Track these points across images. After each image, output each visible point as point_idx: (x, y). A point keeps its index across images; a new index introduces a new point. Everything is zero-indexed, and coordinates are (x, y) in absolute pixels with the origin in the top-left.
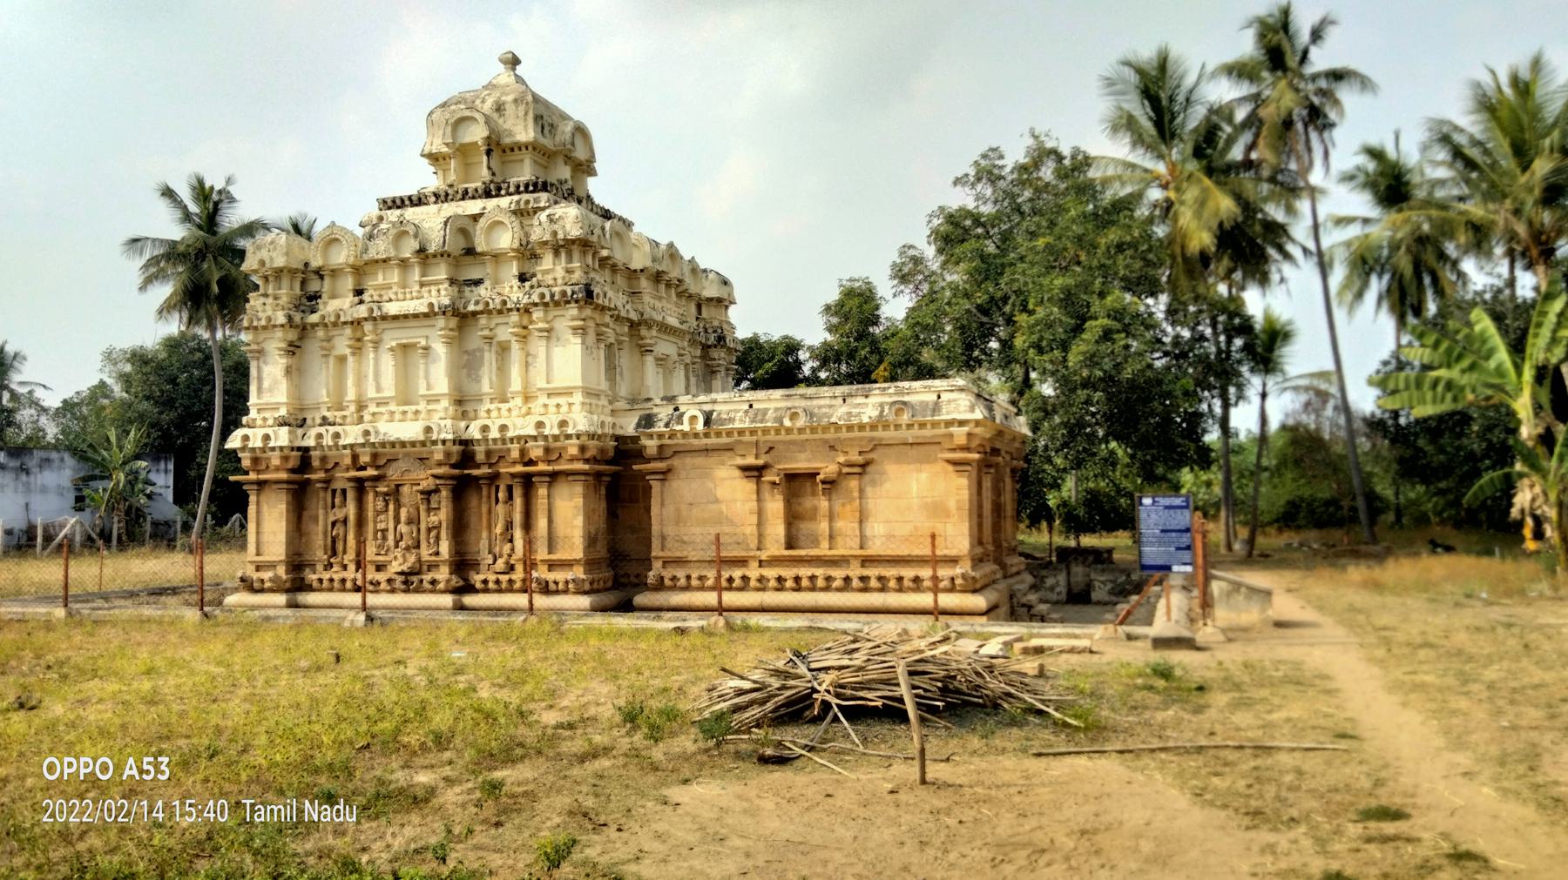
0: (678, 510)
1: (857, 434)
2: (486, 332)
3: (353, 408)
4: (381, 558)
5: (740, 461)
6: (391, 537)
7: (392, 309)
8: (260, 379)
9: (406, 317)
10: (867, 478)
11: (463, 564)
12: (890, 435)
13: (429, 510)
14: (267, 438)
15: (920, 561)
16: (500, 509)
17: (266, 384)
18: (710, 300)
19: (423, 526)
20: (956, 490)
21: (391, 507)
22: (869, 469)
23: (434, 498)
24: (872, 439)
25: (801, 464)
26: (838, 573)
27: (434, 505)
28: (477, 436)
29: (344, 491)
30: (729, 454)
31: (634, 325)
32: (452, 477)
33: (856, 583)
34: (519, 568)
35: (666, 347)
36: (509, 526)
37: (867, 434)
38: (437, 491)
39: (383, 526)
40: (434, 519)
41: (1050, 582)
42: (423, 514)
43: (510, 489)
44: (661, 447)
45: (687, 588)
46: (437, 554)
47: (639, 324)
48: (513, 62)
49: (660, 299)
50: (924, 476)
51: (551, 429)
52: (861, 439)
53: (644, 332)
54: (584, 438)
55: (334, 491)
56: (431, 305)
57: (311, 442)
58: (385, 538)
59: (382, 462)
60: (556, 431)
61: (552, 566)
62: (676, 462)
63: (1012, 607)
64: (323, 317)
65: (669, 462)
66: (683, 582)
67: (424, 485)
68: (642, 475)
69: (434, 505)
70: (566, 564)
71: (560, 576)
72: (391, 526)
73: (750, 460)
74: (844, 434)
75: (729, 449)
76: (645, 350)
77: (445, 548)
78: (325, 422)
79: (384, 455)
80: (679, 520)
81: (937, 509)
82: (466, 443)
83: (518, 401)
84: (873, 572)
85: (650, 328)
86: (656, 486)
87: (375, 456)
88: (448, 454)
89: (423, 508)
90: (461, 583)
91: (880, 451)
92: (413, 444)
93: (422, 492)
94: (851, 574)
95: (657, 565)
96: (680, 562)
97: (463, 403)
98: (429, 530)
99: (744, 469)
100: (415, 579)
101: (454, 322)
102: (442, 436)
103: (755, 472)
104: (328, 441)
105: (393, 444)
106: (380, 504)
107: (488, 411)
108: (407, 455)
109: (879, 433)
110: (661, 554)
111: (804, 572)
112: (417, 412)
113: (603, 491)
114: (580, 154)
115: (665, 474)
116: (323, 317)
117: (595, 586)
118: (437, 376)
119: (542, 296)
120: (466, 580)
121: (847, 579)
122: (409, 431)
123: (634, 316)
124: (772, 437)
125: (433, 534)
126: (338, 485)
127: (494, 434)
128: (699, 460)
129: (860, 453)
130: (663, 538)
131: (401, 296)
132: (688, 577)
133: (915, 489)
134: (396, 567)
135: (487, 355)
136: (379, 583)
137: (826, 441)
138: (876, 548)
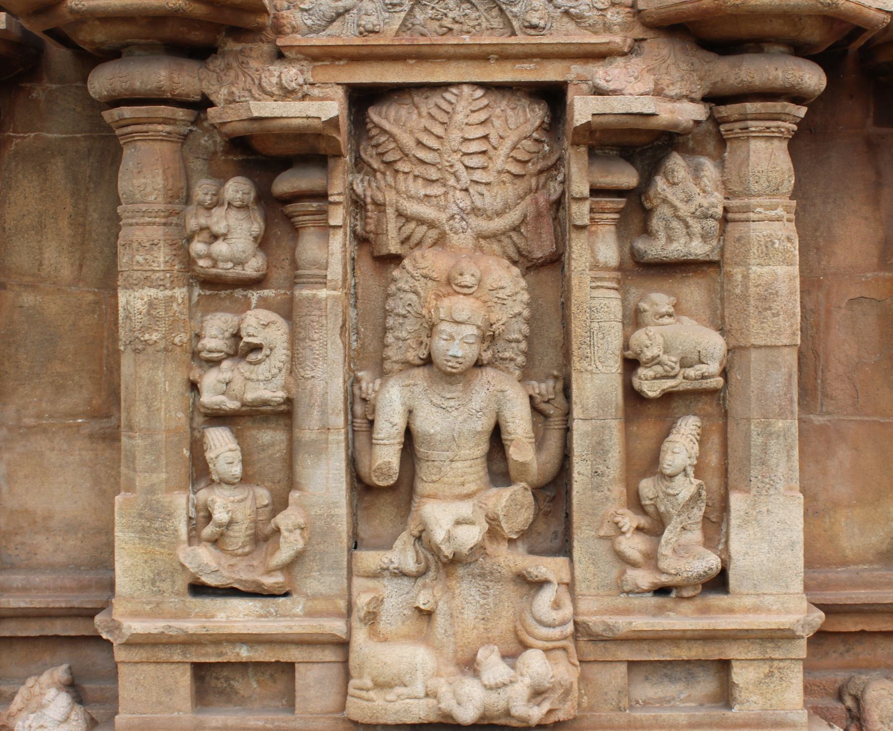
4: (237, 616)
19: (597, 383)
23: (688, 189)
40: (681, 336)
42: (598, 306)
46: (718, 582)
72: (327, 379)
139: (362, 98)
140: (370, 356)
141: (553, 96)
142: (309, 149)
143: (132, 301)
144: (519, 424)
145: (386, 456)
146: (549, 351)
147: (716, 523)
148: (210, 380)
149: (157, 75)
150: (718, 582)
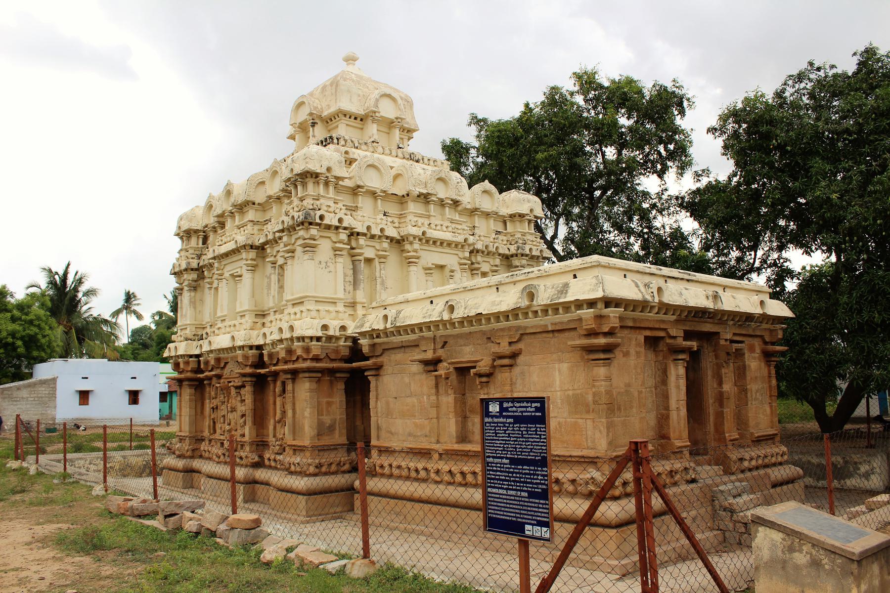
0: (388, 403)
1: (504, 324)
2: (272, 259)
10: (516, 370)
11: (261, 445)
12: (530, 322)
18: (512, 216)
23: (243, 391)
24: (518, 328)
25: (467, 354)
28: (262, 343)
30: (417, 350)
31: (398, 242)
32: (250, 375)
35: (432, 257)
37: (512, 323)
38: (243, 386)
41: (864, 468)
44: (373, 346)
47: (404, 240)
49: (429, 217)
51: (287, 335)
52: (510, 329)
53: (408, 247)
54: (307, 340)
57: (197, 352)
59: (222, 365)
62: (384, 359)
63: (714, 510)
65: (380, 360)
73: (429, 355)
74: (494, 325)
75: (415, 345)
76: (410, 262)
79: (221, 359)
80: (389, 413)
82: (259, 348)
85: (411, 243)
87: (218, 360)
88: (246, 357)
90: (257, 459)
91: (527, 339)
95: (374, 453)
101: (252, 254)
103: (432, 364)
107: (271, 322)
109: (522, 322)
112: (235, 326)
113: (341, 386)
114: (387, 111)
115: (378, 368)
117: (324, 469)
120: (261, 457)
123: (391, 232)
124: (442, 332)
128: (398, 356)
129: (510, 343)
130: (378, 428)
132: (391, 466)
133: (558, 383)
137: (483, 333)
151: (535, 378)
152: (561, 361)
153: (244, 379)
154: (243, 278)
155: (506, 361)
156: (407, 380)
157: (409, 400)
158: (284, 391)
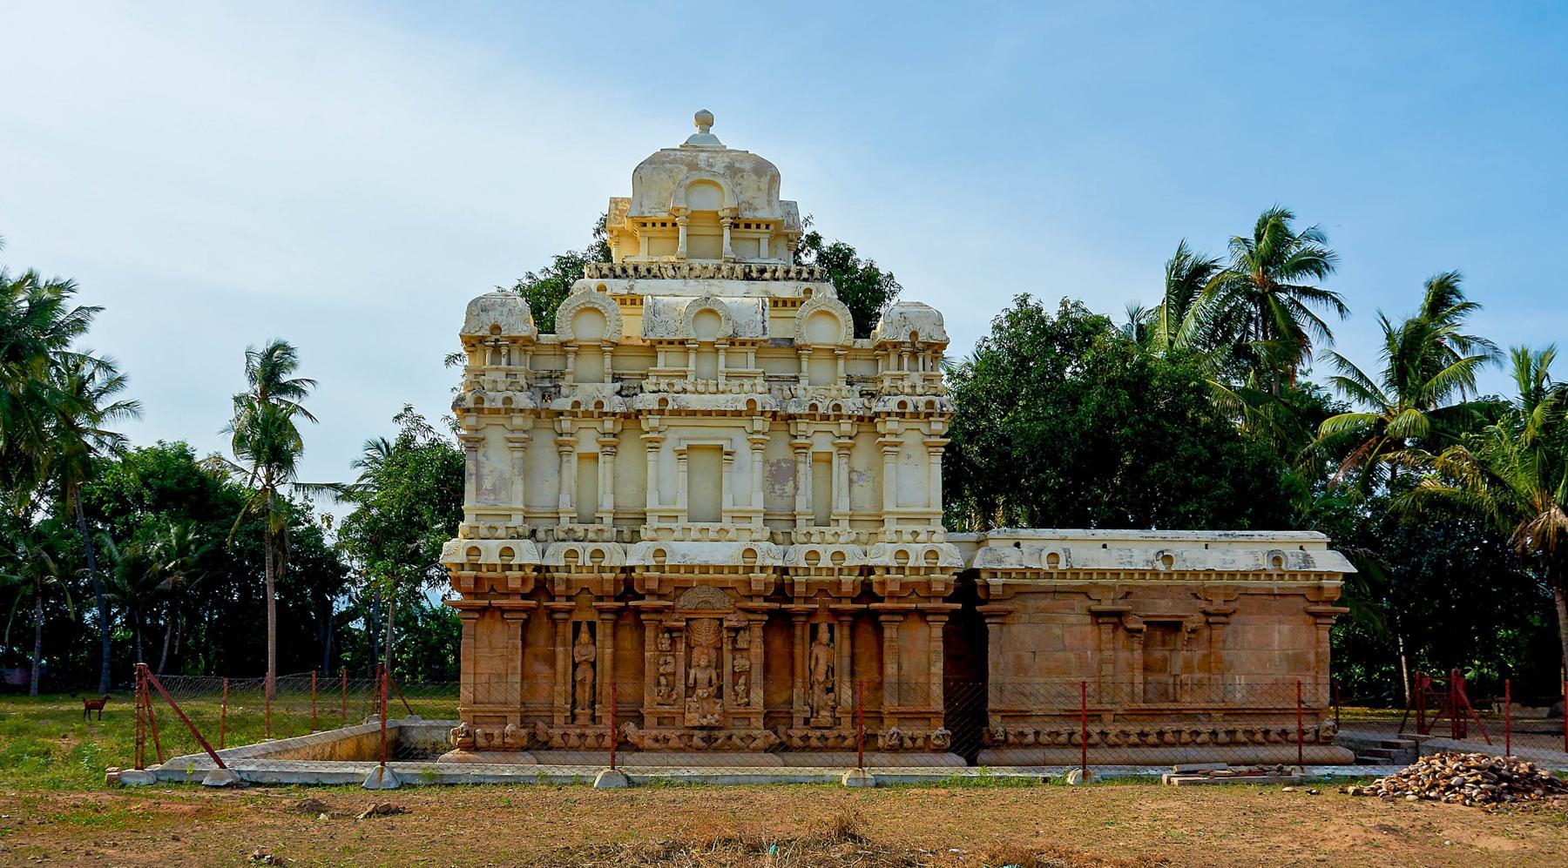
3: (608, 520)
5: (1096, 607)
6: (681, 687)
7: (693, 402)
8: (479, 478)
9: (708, 413)
10: (1229, 629)
13: (735, 650)
14: (507, 552)
15: (1284, 713)
16: (821, 652)
17: (487, 484)
19: (727, 669)
20: (1318, 642)
21: (681, 646)
22: (1233, 618)
24: (1238, 588)
26: (1205, 728)
27: (741, 644)
29: (592, 626)
32: (769, 612)
33: (1222, 737)
34: (847, 721)
36: (831, 670)
38: (747, 628)
39: (669, 669)
40: (742, 663)
42: (728, 657)
43: (831, 629)
45: (1037, 744)
46: (748, 704)
48: (705, 120)
50: (1286, 628)
55: (577, 626)
56: (751, 402)
58: (672, 687)
60: (923, 563)
61: (904, 717)
64: (577, 404)
66: (1031, 738)
67: (733, 621)
68: (982, 617)
69: (741, 644)
70: (925, 717)
71: (917, 730)
73: (1106, 606)
77: (757, 696)
78: (570, 535)
80: (1020, 668)
81: (1297, 662)
83: (845, 524)
84: (1240, 726)
86: (993, 629)
89: (727, 647)
92: (720, 569)
93: (729, 629)
94: (1218, 728)
96: (1023, 716)
97: (782, 524)
98: (735, 675)
99: (1096, 615)
100: (722, 734)
102: (769, 562)
104: (585, 559)
105: (690, 569)
106: (666, 645)
108: (703, 582)
109: (1251, 583)
110: (1002, 707)
111: (1169, 727)
116: (577, 404)
118: (745, 485)
119: (902, 404)
121: (1214, 733)
122: (723, 553)
125: (742, 681)
126: (583, 616)
127: (826, 562)
128: (1045, 602)
131: (701, 388)
134: (693, 719)
135: (801, 467)
136: (666, 740)
137: (1188, 588)
138: (1239, 698)
139: (688, 620)
140: (688, 666)
141: (721, 620)
142: (679, 630)
143: (647, 654)
144: (714, 677)
145: (691, 681)
146: (719, 665)
147: (748, 695)
148: (661, 670)
149: (654, 616)
150: (748, 704)
151: (1250, 636)
152: (1280, 623)
153: (752, 617)
154: (735, 457)
155: (1223, 619)
156: (1057, 631)
157: (1060, 655)
158: (832, 639)
